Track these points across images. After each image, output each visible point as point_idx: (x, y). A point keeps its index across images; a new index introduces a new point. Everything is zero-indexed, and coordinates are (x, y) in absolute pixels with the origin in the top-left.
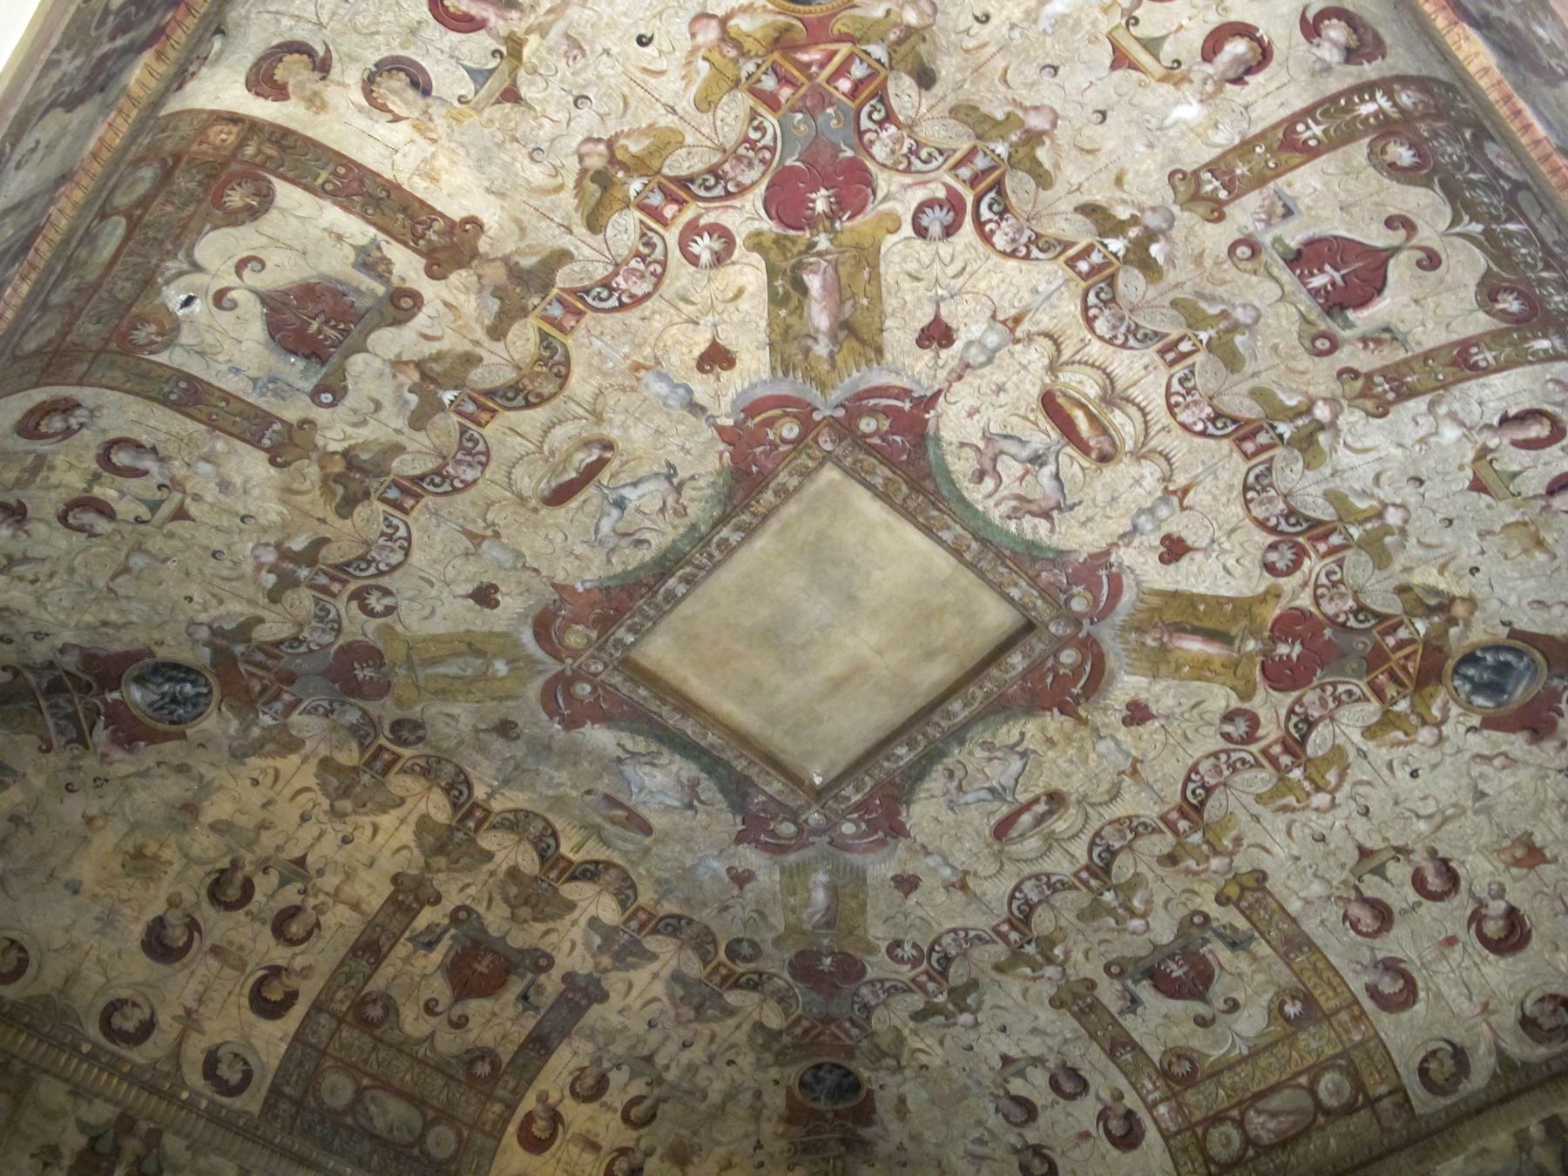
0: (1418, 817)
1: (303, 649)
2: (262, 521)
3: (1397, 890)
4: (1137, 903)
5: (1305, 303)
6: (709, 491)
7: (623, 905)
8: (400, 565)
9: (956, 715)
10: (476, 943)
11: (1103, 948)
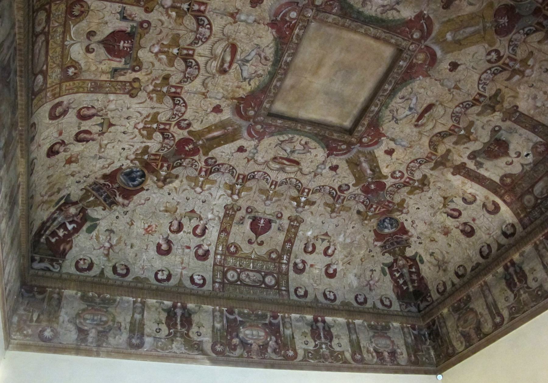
2: (526, 85)
4: (163, 57)
5: (260, 215)
6: (384, 119)
8: (483, 73)
9: (277, 81)
11: (158, 29)
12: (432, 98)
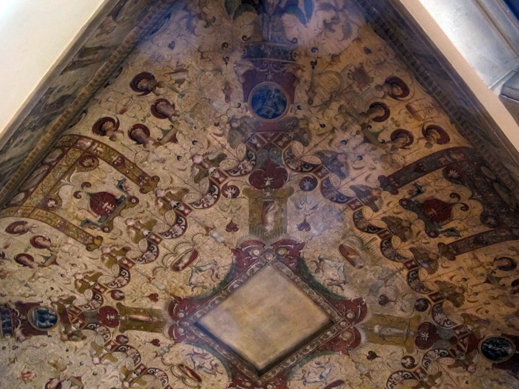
1: (441, 351)
4: (134, 232)
7: (361, 212)
8: (395, 373)
9: (217, 299)
10: (432, 220)
12: (344, 376)
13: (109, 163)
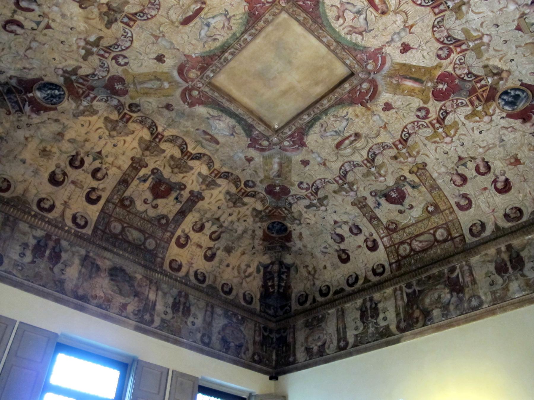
0: (480, 147)
1: (96, 78)
2: (79, 30)
3: (470, 172)
4: (382, 172)
6: (240, 21)
7: (209, 168)
9: (325, 105)
11: (370, 186)
12: (183, 31)
13: (380, 221)
